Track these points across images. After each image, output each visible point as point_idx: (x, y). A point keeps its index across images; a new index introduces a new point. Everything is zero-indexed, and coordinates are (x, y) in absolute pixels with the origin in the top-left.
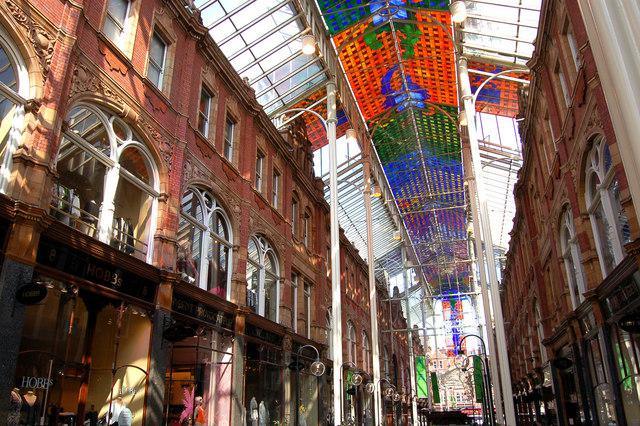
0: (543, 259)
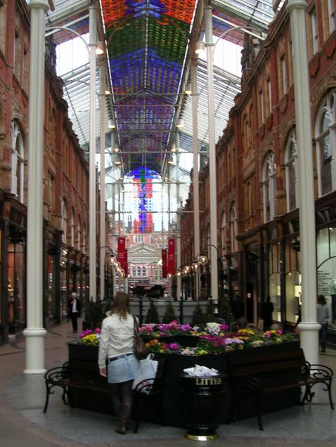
0: (246, 174)
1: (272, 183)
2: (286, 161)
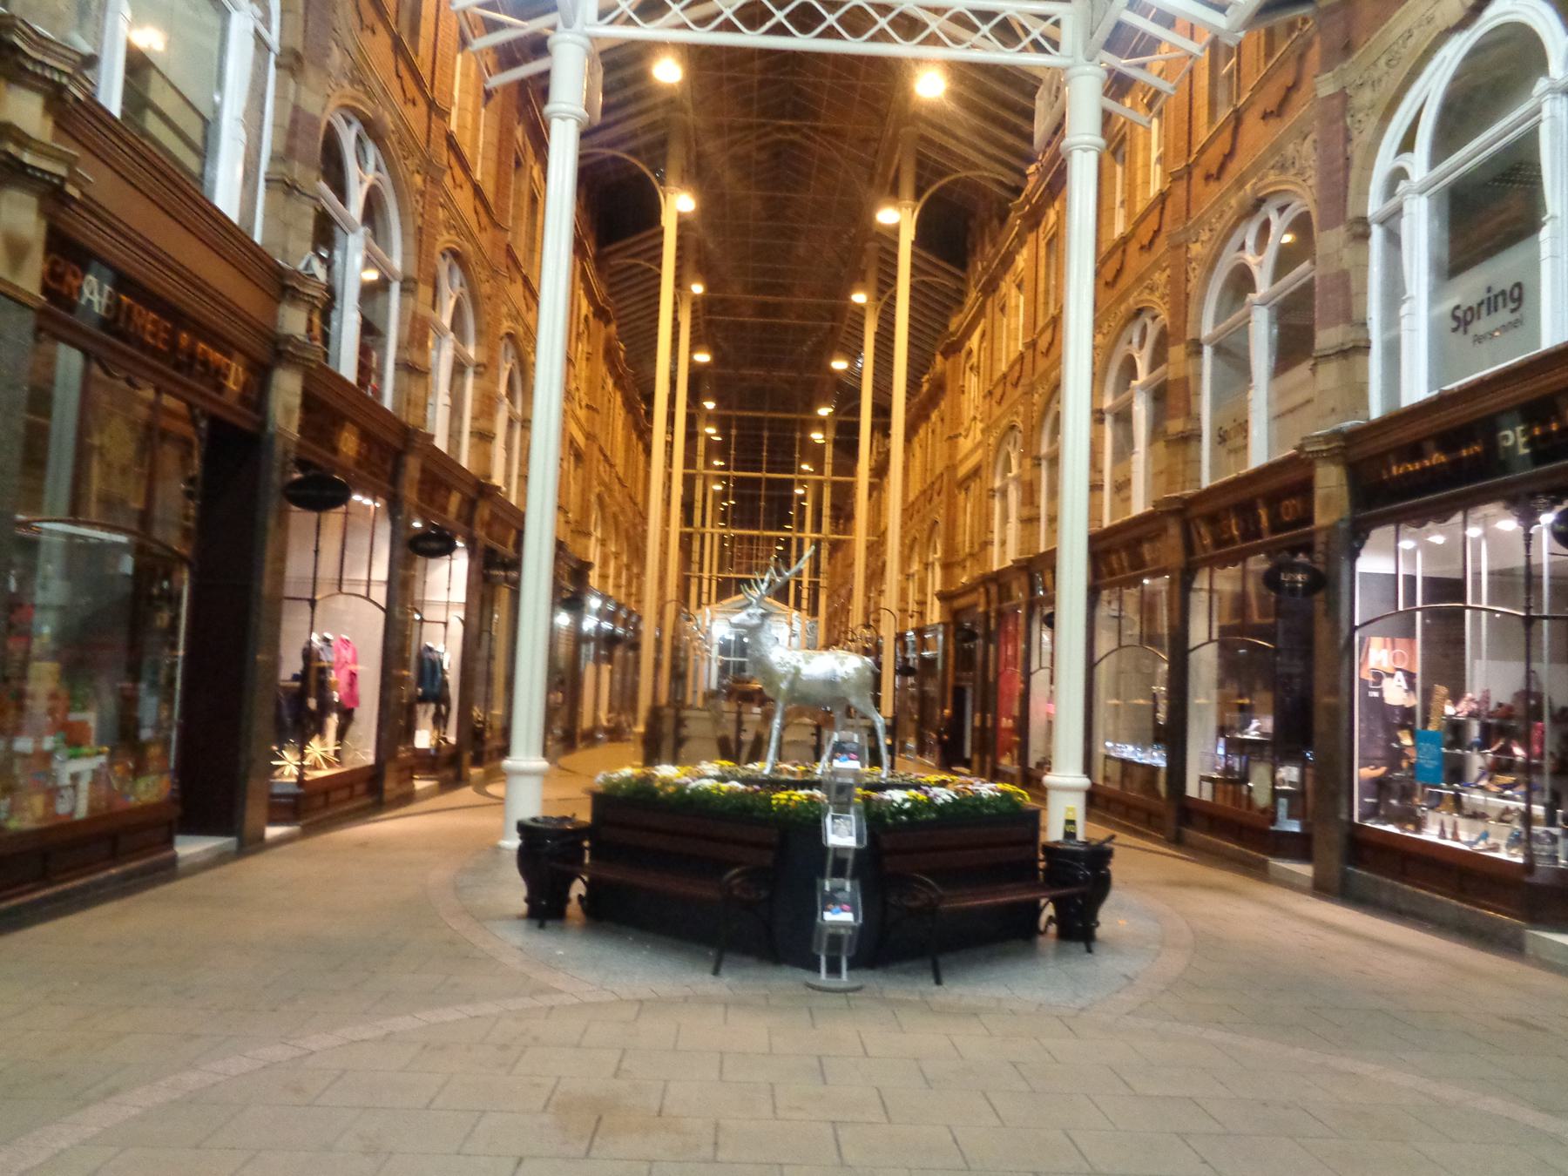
0: (963, 471)
1: (1014, 496)
2: (1044, 449)
